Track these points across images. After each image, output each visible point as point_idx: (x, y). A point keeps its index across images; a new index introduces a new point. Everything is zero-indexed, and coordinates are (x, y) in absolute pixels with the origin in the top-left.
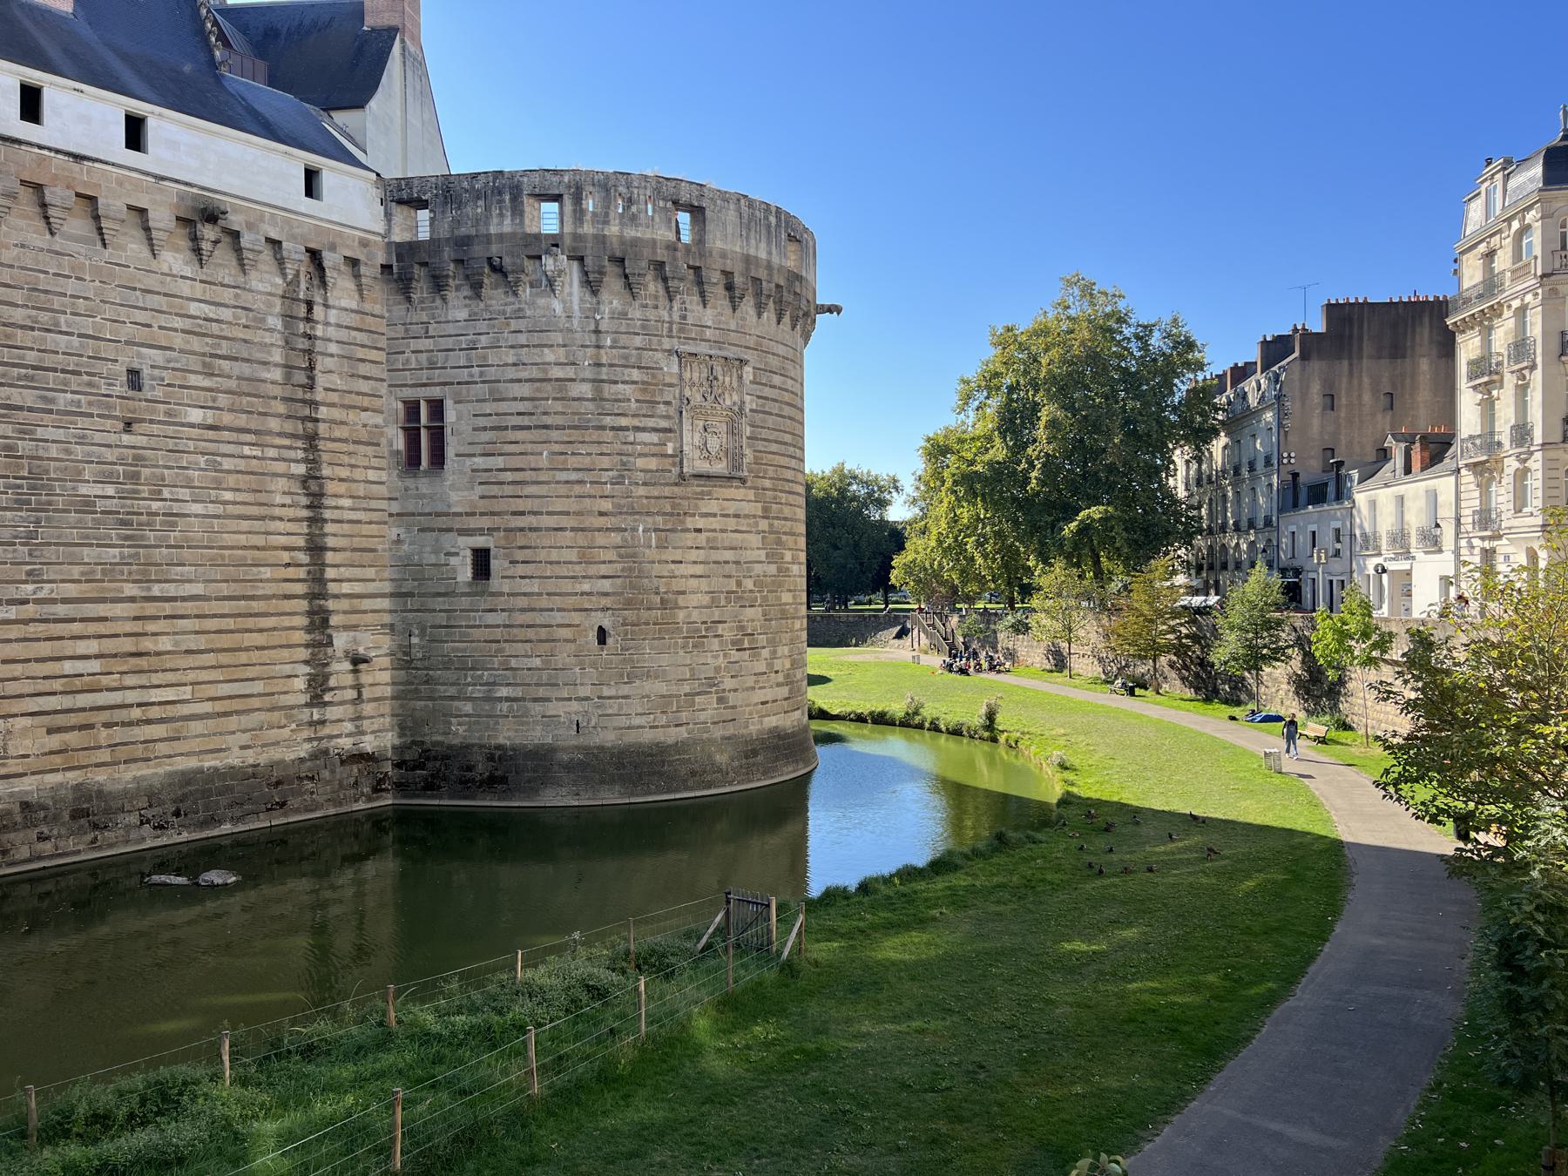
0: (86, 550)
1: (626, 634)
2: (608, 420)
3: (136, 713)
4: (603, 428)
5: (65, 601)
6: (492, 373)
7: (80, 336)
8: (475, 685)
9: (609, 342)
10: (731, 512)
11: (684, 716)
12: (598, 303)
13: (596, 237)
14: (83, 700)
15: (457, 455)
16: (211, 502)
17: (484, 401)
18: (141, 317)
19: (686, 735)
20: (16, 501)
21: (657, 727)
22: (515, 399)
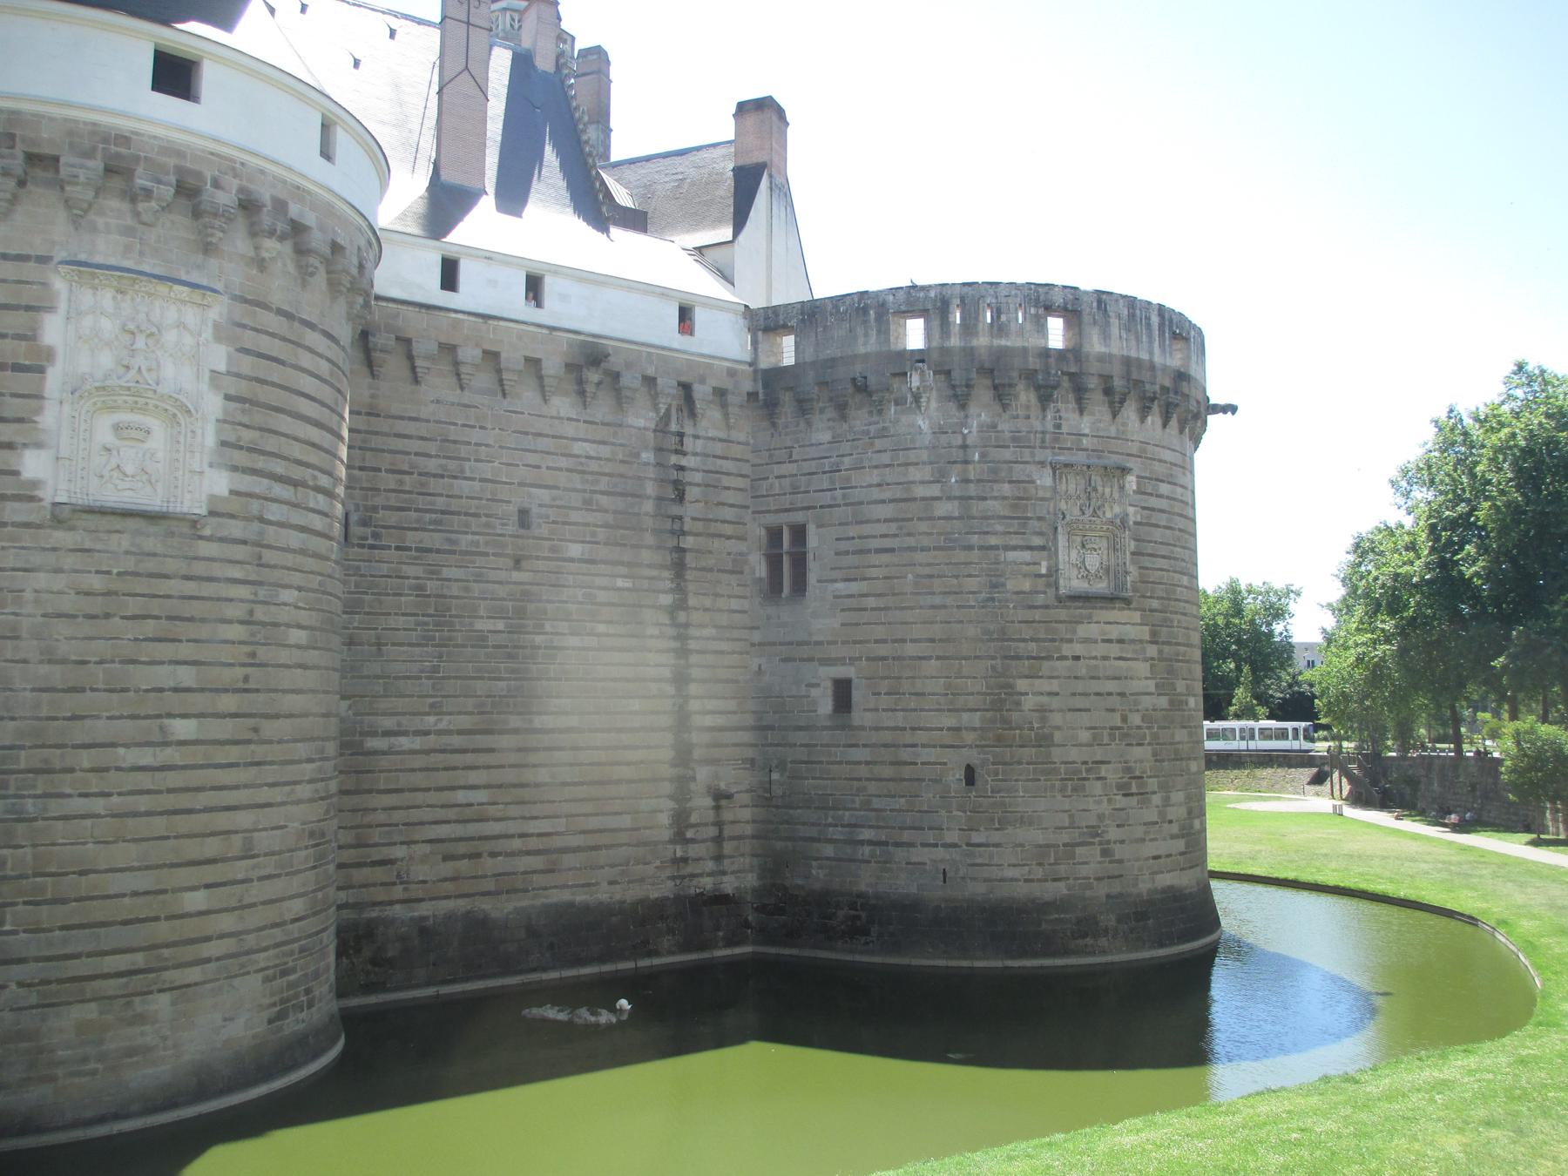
0: (479, 684)
1: (997, 774)
2: (975, 540)
3: (517, 844)
4: (970, 548)
5: (460, 732)
6: (857, 495)
7: (482, 480)
8: (836, 826)
9: (977, 457)
10: (1114, 636)
11: (1062, 869)
12: (966, 417)
13: (964, 349)
14: (472, 829)
15: (819, 581)
16: (588, 634)
17: (846, 524)
18: (532, 459)
19: (1065, 892)
20: (424, 638)
21: (1032, 881)
22: (879, 521)
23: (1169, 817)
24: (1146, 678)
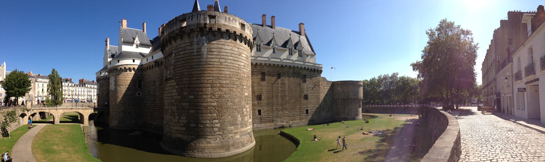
1: (166, 111)
10: (170, 85)
23: (180, 122)
24: (176, 93)
